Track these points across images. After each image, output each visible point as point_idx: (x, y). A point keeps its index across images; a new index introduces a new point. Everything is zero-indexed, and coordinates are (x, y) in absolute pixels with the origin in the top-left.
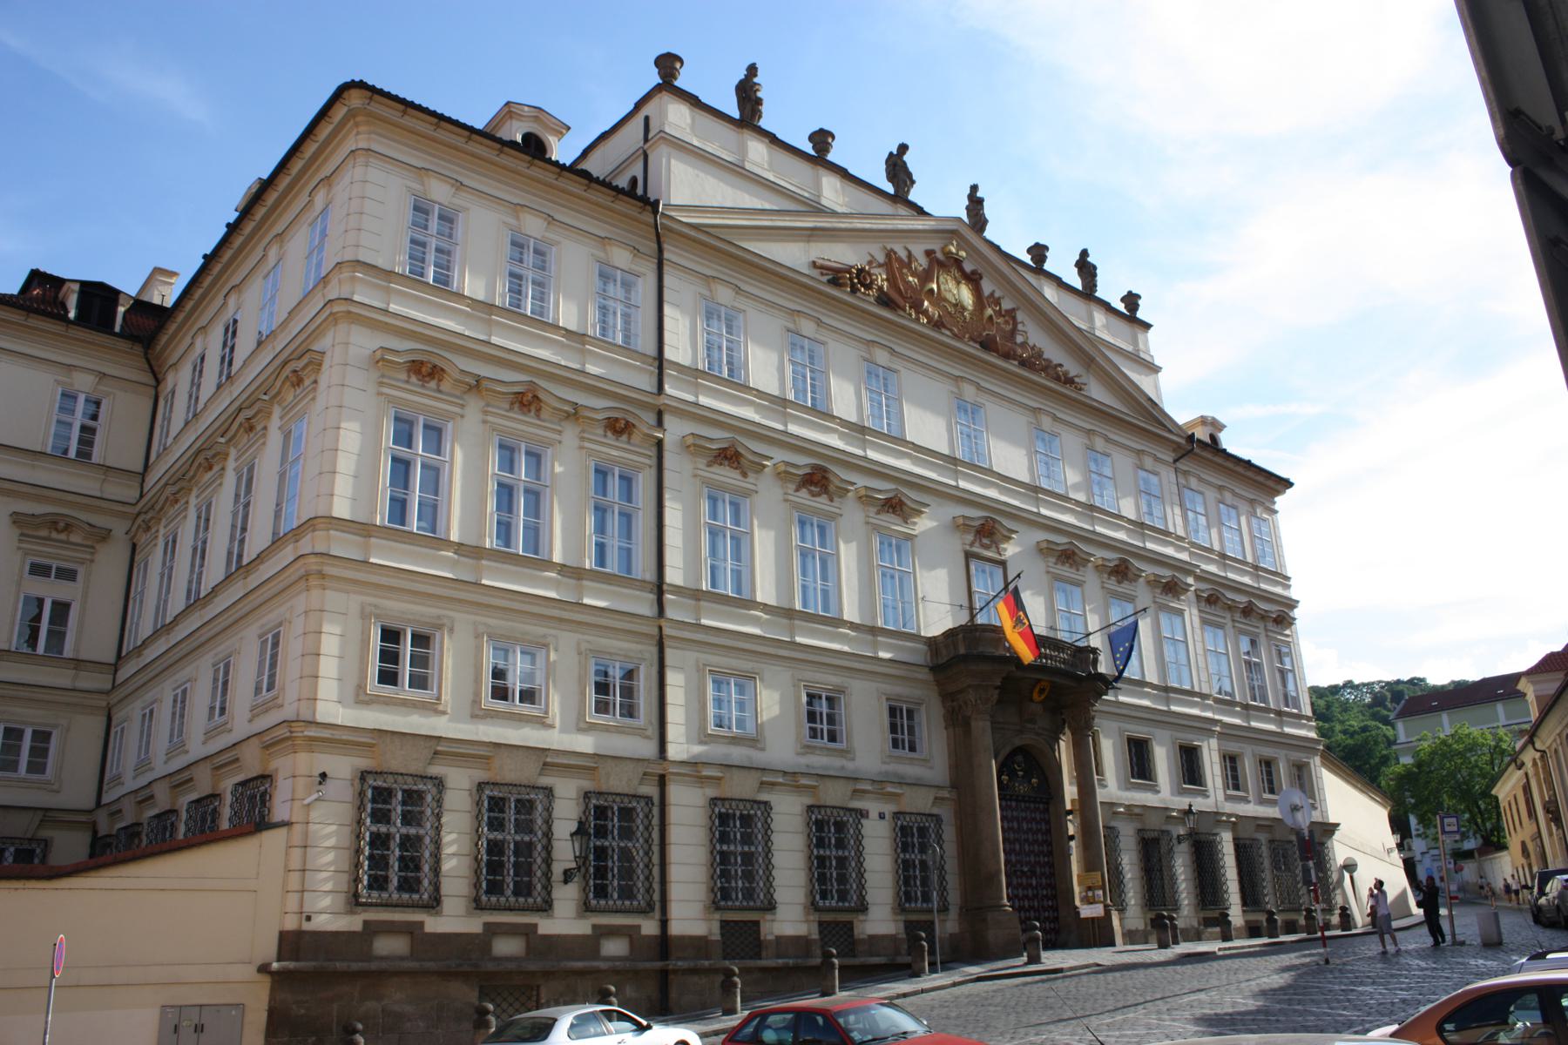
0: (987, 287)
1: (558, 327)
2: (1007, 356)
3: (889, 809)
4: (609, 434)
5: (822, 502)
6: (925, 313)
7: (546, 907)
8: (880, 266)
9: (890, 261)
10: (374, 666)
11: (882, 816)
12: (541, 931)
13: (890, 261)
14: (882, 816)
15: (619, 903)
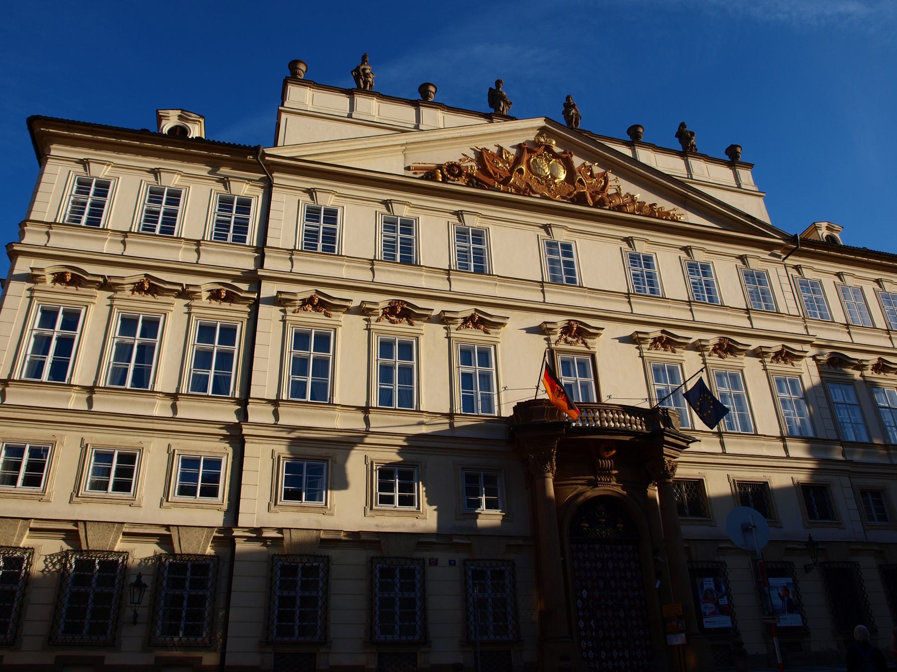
0: (577, 161)
1: (181, 238)
2: (599, 204)
3: (459, 557)
4: (214, 302)
5: (403, 327)
6: (514, 185)
7: (113, 645)
8: (472, 160)
9: (481, 156)
10: (88, 476)
11: (452, 563)
12: (106, 662)
13: (481, 156)
14: (452, 563)
15: (184, 639)
